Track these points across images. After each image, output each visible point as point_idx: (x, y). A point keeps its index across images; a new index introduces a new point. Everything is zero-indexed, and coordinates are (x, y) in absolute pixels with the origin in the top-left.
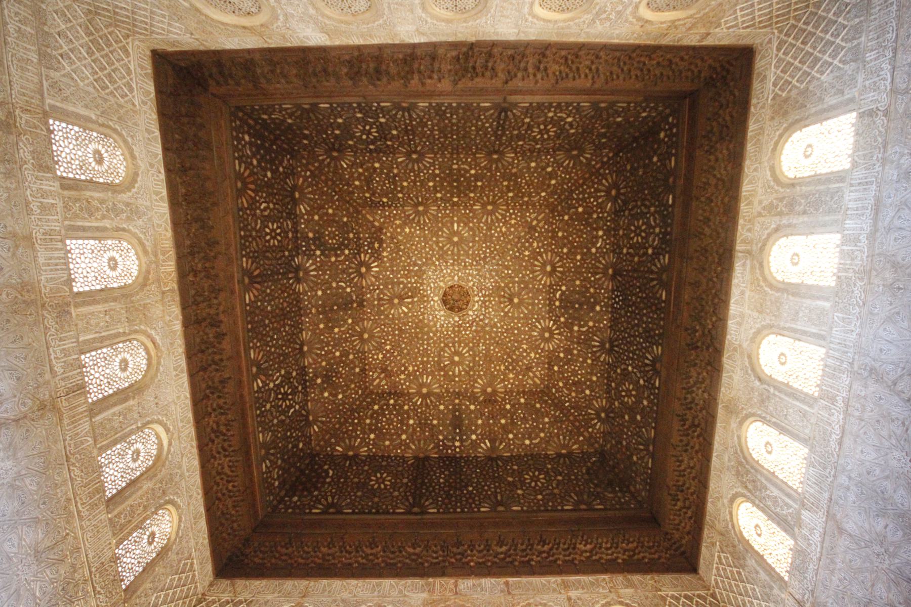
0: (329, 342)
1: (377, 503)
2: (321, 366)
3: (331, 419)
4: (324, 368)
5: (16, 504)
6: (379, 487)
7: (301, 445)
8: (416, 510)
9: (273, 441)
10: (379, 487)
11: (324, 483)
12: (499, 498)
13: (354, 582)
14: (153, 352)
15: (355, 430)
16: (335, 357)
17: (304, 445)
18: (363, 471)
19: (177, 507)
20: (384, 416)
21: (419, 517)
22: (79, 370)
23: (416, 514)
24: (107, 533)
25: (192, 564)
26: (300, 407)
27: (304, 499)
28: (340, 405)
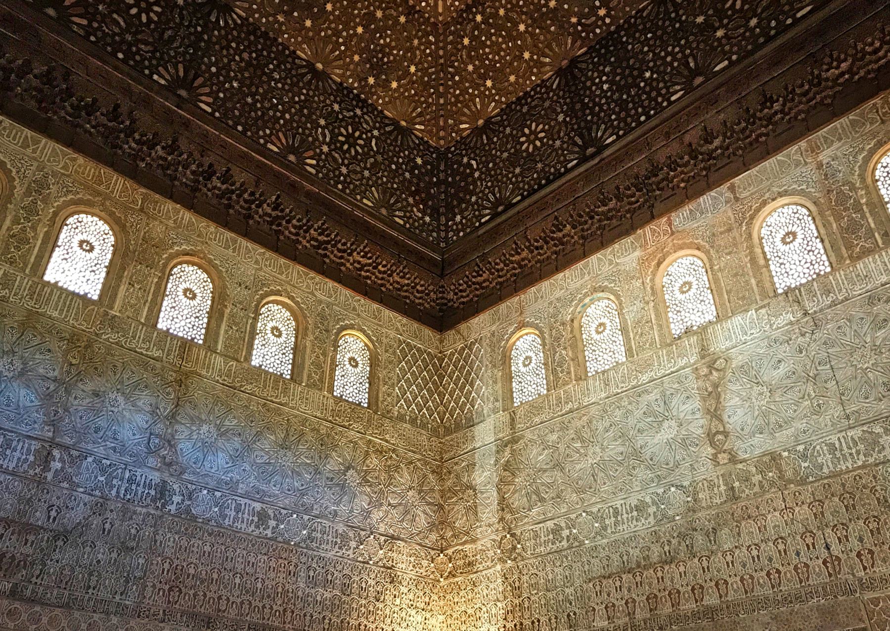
0: (336, 29)
1: (543, 170)
2: (357, 64)
3: (426, 102)
4: (363, 61)
5: (236, 439)
6: (535, 146)
7: (419, 161)
8: (590, 151)
9: (384, 192)
10: (535, 146)
11: (474, 182)
12: (692, 65)
13: (561, 275)
14: (196, 260)
15: (464, 91)
16: (361, 38)
17: (422, 157)
18: (507, 137)
19: (351, 327)
20: (484, 45)
21: (596, 160)
22: (169, 338)
23: (593, 156)
24: (314, 394)
25: (408, 344)
26: (379, 129)
27: (466, 213)
28: (422, 77)
